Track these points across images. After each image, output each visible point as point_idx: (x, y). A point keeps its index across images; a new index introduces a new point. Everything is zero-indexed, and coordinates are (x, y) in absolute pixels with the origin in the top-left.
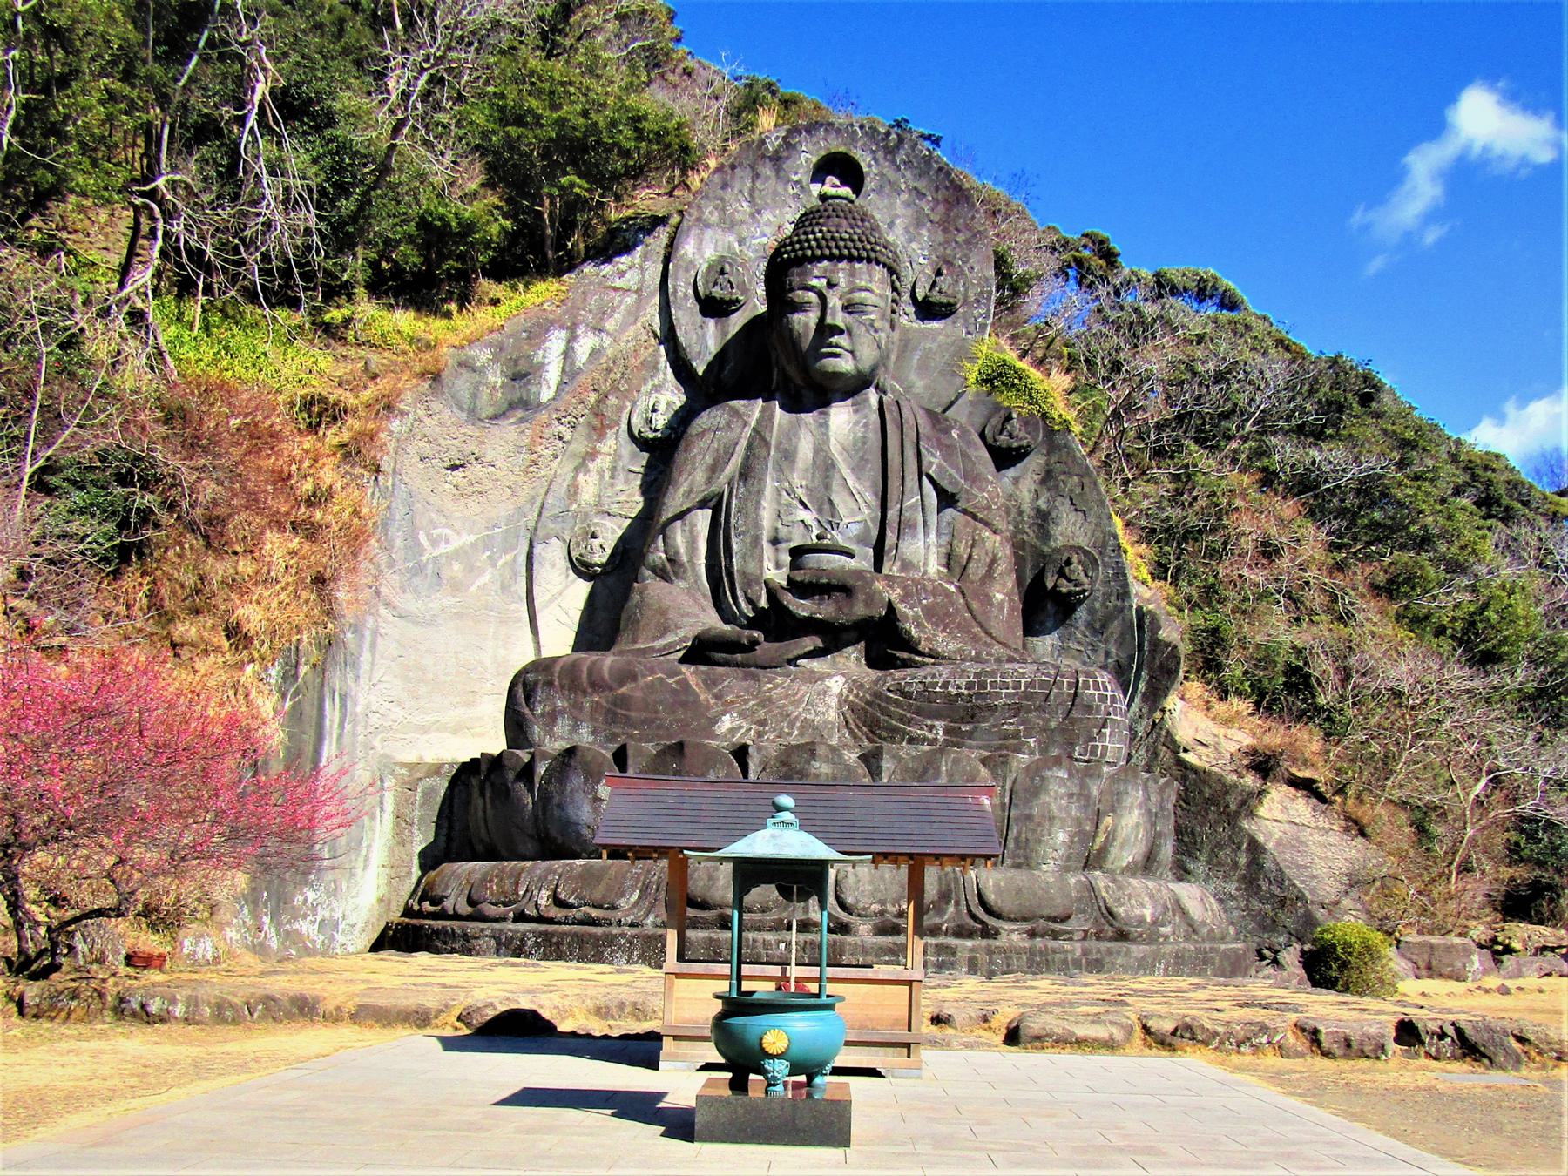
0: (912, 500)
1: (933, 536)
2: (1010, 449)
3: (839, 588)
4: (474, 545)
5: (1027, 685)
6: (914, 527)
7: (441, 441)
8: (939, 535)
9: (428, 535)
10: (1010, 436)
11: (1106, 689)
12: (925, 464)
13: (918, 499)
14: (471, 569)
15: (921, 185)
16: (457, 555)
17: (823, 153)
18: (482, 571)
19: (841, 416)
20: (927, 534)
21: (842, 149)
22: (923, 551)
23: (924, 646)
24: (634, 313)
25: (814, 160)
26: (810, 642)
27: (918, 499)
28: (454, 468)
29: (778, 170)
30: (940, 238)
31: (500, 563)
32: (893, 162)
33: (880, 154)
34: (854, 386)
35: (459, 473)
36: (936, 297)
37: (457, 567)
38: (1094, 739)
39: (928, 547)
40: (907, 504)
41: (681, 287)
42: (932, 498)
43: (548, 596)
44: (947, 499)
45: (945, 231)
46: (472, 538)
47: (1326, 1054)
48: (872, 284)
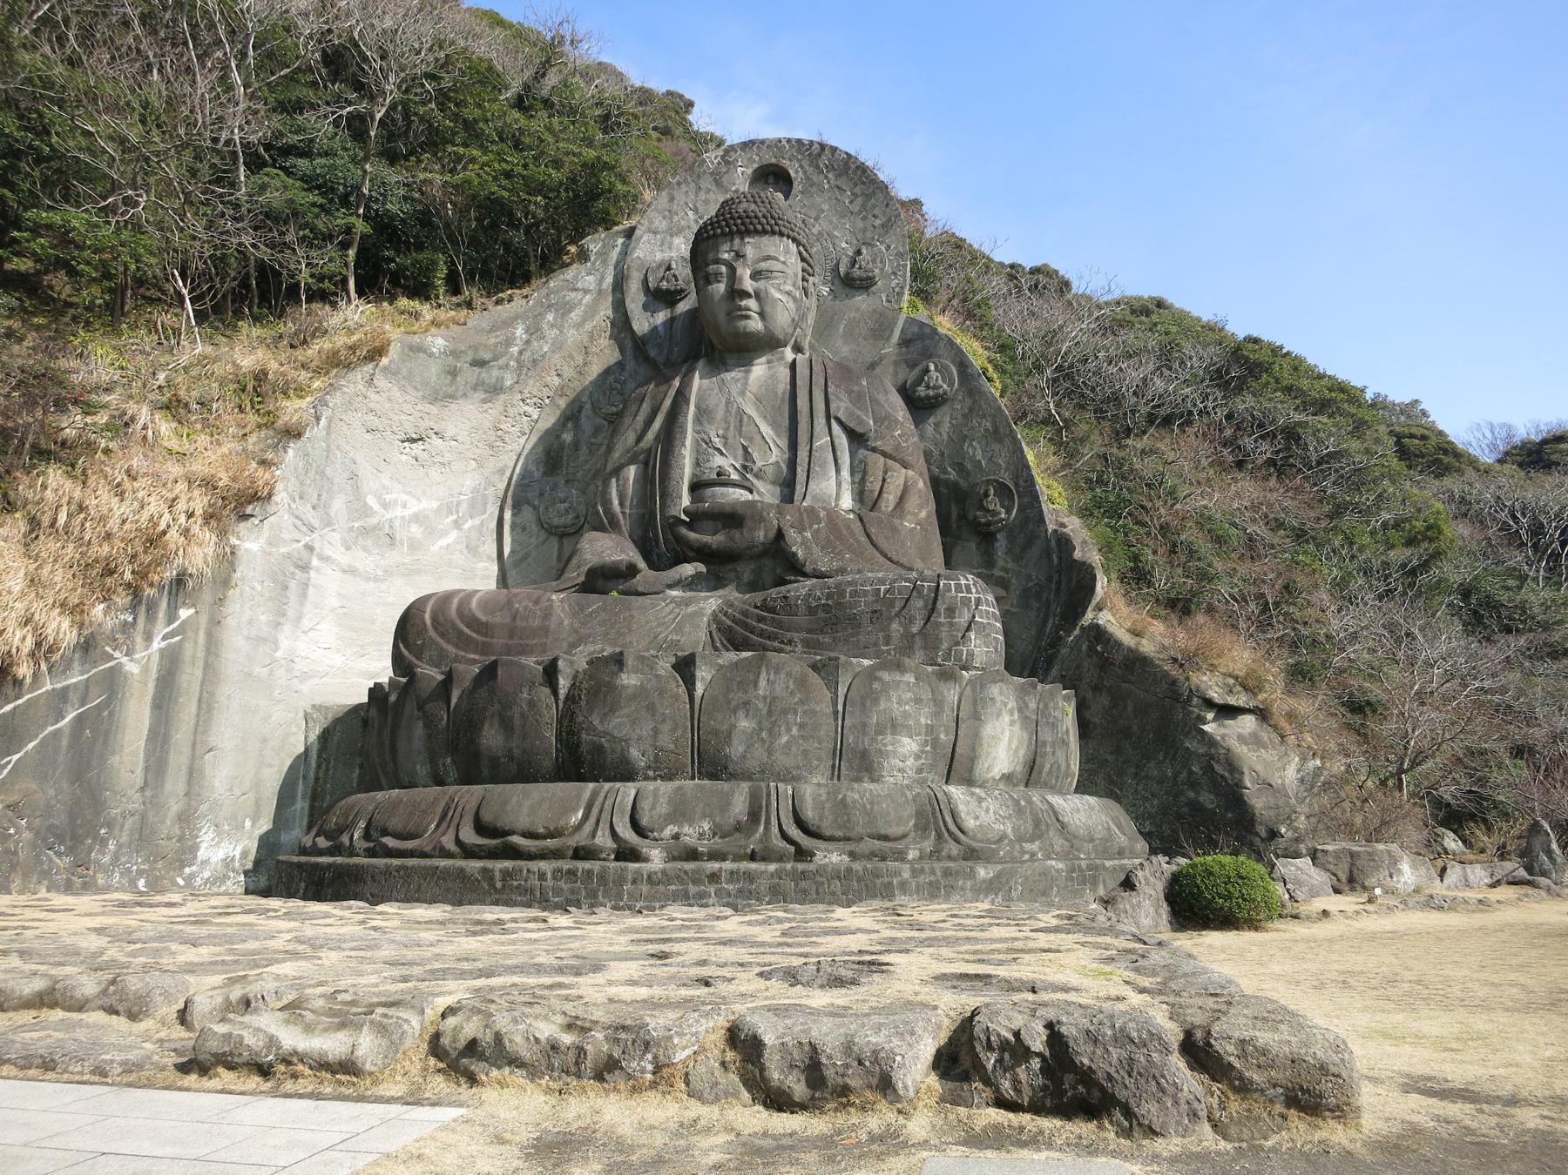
0: (822, 441)
1: (845, 473)
2: (928, 397)
3: (731, 519)
4: (438, 511)
5: (887, 591)
6: (823, 465)
7: (391, 415)
8: (852, 473)
9: (379, 498)
10: (928, 387)
11: (969, 591)
12: (833, 406)
13: (827, 440)
14: (431, 532)
15: (841, 182)
16: (416, 518)
17: (756, 166)
18: (444, 533)
19: (759, 369)
20: (838, 471)
21: (774, 160)
22: (833, 489)
23: (808, 569)
24: (592, 311)
25: (750, 171)
27: (827, 440)
28: (413, 441)
29: (718, 183)
30: (860, 224)
31: (466, 526)
32: (817, 167)
33: (805, 163)
34: (769, 343)
35: (419, 446)
36: (856, 272)
37: (415, 529)
38: (957, 644)
39: (839, 484)
40: (816, 444)
42: (842, 440)
44: (857, 438)
45: (864, 219)
46: (435, 505)
47: (777, 1101)
48: (784, 253)
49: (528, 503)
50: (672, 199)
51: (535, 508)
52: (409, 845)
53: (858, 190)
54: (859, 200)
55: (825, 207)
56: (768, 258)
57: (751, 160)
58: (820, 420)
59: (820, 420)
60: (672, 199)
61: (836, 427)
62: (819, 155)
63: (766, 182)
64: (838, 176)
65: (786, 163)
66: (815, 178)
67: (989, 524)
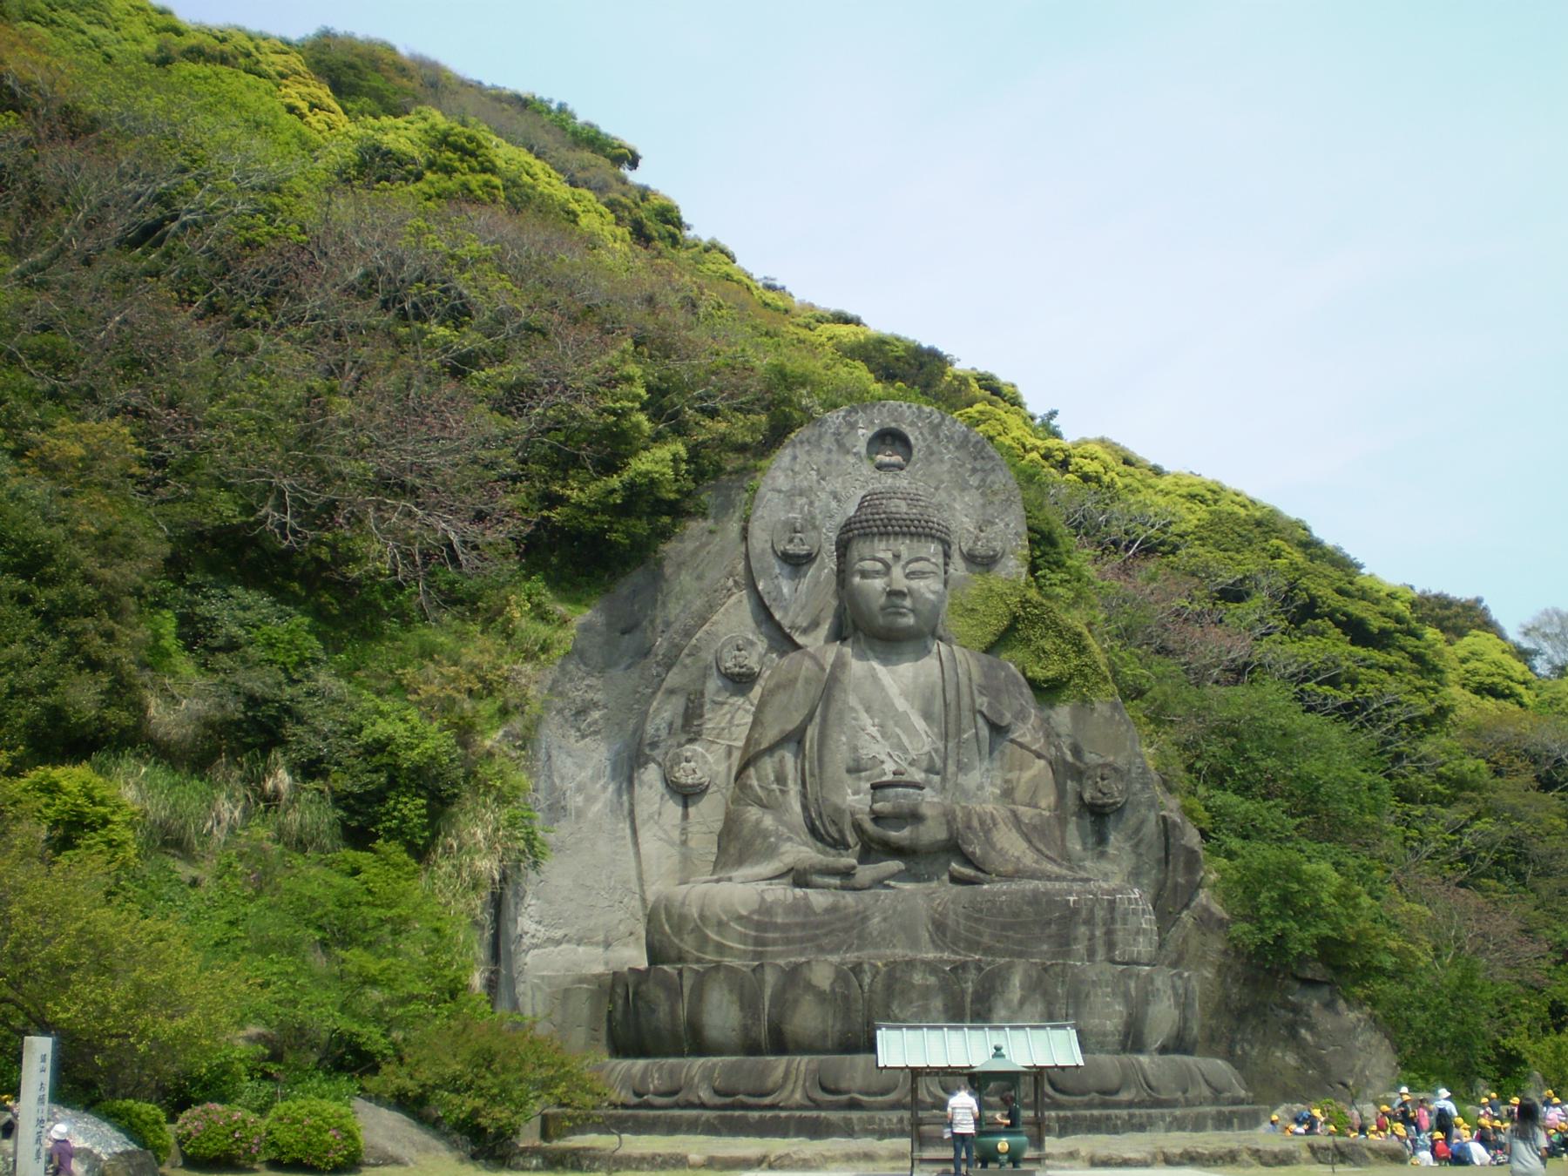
14: (590, 799)
21: (893, 425)
26: (895, 865)
29: (841, 445)
32: (937, 436)
33: (926, 431)
41: (760, 539)
42: (985, 732)
43: (645, 816)
49: (654, 760)
50: (795, 458)
51: (660, 765)
52: (767, 1100)
53: (978, 465)
54: (979, 475)
55: (946, 477)
56: (918, 560)
57: (872, 422)
58: (966, 713)
59: (966, 713)
60: (795, 458)
61: (980, 721)
62: (940, 425)
63: (883, 443)
64: (957, 448)
65: (906, 429)
66: (935, 447)
67: (1104, 806)
